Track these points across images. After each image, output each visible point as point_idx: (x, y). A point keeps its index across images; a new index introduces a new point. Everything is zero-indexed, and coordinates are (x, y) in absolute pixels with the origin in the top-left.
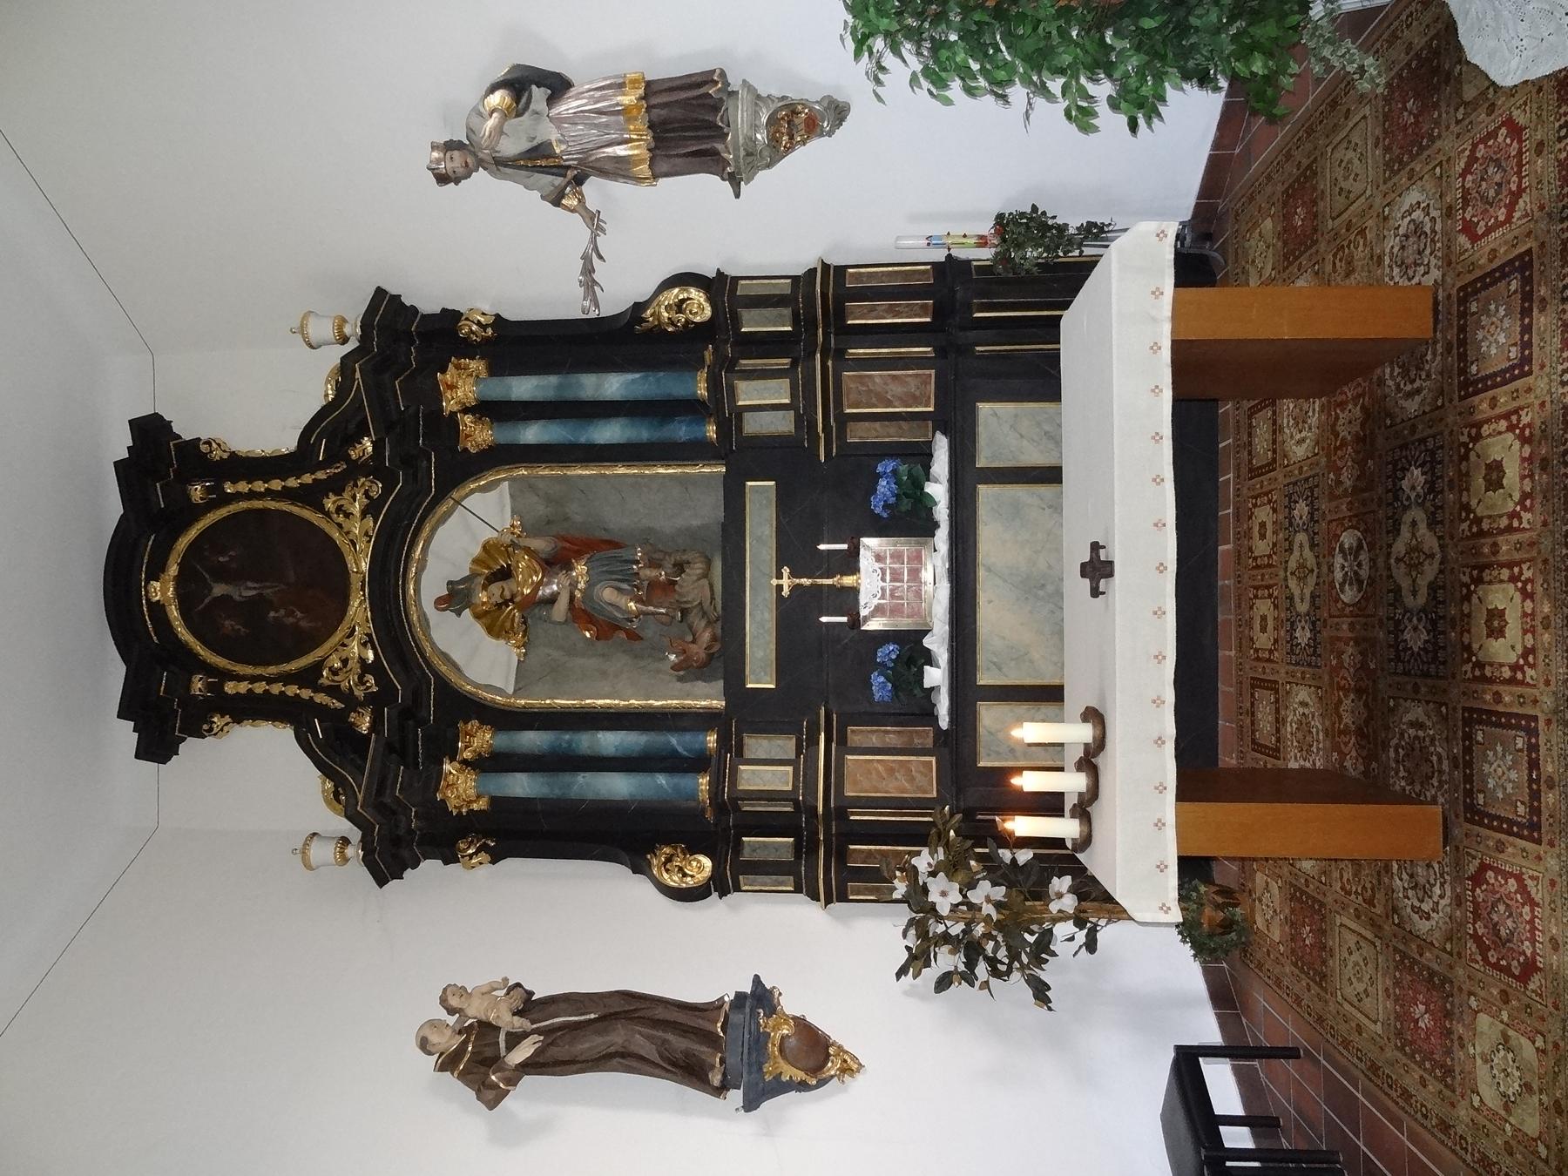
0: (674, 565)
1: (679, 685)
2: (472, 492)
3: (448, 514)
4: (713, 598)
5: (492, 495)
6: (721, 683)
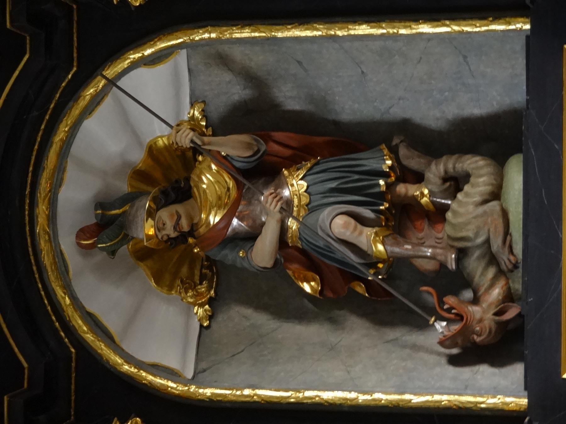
0: (445, 180)
1: (452, 370)
2: (134, 65)
3: (97, 100)
4: (507, 232)
5: (163, 68)
6: (516, 372)
